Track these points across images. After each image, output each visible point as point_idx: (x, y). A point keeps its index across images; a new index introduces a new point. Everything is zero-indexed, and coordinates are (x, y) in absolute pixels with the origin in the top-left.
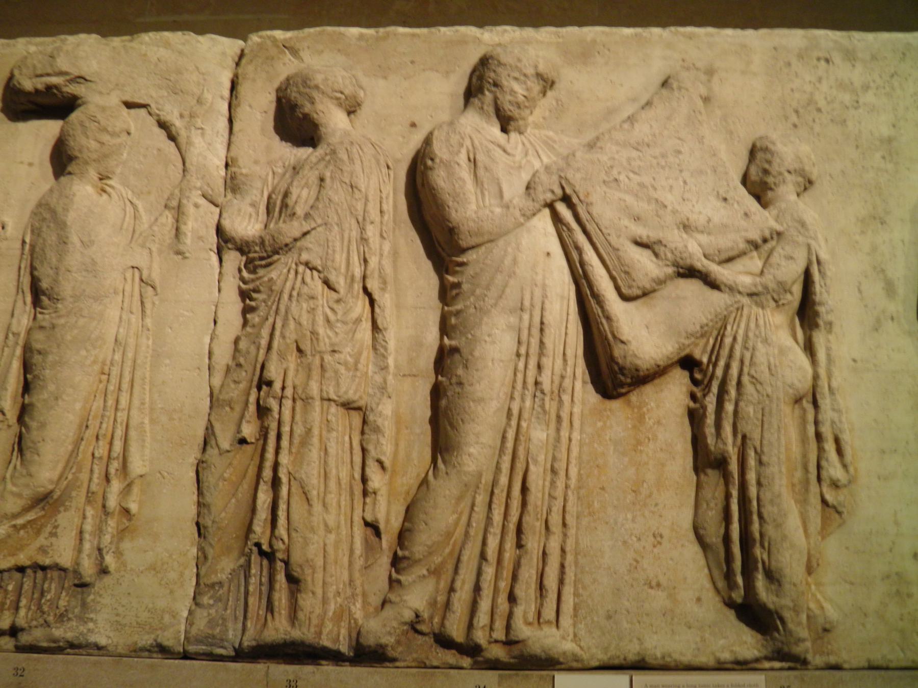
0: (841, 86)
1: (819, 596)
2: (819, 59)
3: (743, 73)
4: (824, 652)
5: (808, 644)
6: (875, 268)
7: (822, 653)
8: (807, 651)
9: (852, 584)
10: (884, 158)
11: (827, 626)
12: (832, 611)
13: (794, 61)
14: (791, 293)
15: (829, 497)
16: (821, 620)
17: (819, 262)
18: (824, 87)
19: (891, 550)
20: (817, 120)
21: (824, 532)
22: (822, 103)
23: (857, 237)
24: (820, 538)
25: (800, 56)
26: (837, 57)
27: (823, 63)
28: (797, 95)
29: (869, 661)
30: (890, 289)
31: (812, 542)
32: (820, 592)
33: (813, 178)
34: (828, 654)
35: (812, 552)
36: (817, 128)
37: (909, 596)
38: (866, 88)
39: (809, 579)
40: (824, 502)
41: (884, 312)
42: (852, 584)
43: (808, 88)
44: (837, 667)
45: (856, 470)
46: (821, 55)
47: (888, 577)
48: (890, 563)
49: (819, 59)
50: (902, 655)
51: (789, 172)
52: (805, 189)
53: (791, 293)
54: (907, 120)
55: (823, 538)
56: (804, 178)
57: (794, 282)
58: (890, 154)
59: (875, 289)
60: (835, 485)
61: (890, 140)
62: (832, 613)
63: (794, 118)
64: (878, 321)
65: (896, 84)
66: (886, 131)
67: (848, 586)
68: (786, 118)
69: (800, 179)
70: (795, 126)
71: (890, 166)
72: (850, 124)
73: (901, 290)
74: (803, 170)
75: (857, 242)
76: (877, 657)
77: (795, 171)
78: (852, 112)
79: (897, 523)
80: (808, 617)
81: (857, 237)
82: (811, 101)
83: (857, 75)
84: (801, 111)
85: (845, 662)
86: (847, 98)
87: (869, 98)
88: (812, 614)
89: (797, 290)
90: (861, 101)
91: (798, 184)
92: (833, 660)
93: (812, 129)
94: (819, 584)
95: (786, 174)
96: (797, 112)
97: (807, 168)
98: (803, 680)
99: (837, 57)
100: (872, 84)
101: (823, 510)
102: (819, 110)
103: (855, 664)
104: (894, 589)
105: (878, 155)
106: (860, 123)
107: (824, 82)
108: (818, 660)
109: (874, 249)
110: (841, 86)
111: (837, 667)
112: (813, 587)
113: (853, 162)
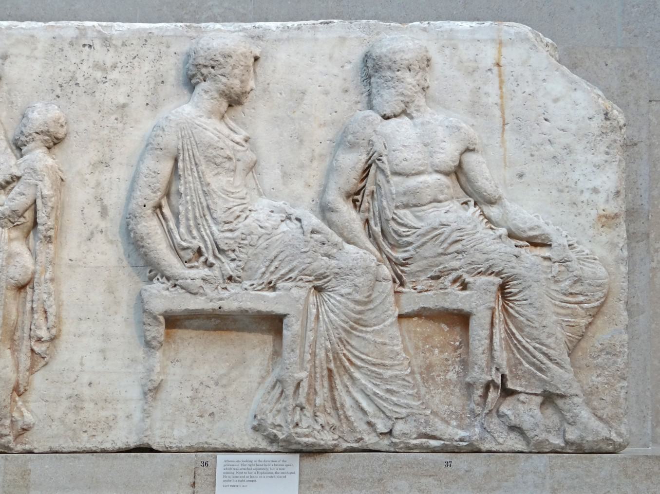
0: (97, 66)
1: (23, 409)
2: (84, 45)
3: (28, 57)
4: (22, 443)
5: (11, 438)
6: (96, 198)
7: (22, 443)
8: (9, 442)
9: (47, 401)
10: (116, 119)
11: (25, 427)
12: (31, 418)
13: (66, 47)
14: (24, 217)
15: (36, 349)
16: (20, 424)
17: (42, 197)
18: (84, 67)
19: (75, 381)
20: (74, 92)
21: (32, 370)
22: (80, 80)
23: (88, 176)
24: (28, 373)
25: (71, 44)
26: (97, 44)
27: (87, 47)
28: (63, 74)
29: (51, 448)
30: (104, 212)
31: (21, 375)
32: (26, 406)
33: (60, 136)
34: (26, 444)
35: (20, 382)
36: (73, 100)
37: (82, 409)
38: (114, 67)
39: (17, 398)
40: (32, 351)
41: (97, 227)
42: (47, 401)
43: (73, 68)
44: (31, 452)
45: (60, 330)
46: (86, 42)
47: (70, 397)
48: (73, 389)
49: (84, 45)
50: (72, 444)
51: (37, 133)
52: (55, 144)
53: (24, 217)
54: (138, 91)
55: (32, 374)
56: (50, 136)
57: (26, 210)
58: (122, 117)
59: (93, 212)
60: (39, 340)
61: (124, 106)
62: (29, 418)
63: (58, 91)
64: (92, 233)
65: (136, 64)
66: (122, 100)
67: (44, 403)
68: (53, 91)
69: (47, 138)
70: (59, 97)
71: (120, 125)
72: (96, 94)
73: (112, 213)
74: (48, 131)
75: (87, 180)
76: (56, 446)
77: (42, 132)
78: (101, 85)
79: (82, 364)
80: (12, 421)
81: (88, 176)
82: (72, 78)
83: (109, 58)
84: (64, 85)
85: (35, 448)
86: (99, 75)
87: (114, 75)
88: (14, 420)
89: (29, 215)
90: (108, 78)
91: (46, 141)
92: (27, 447)
93: (69, 99)
94: (25, 402)
95: (35, 135)
96: (61, 86)
97: (51, 130)
98: (7, 459)
99: (97, 44)
100: (119, 65)
101: (32, 355)
102: (77, 84)
103: (41, 450)
104: (73, 404)
105: (113, 117)
106: (105, 94)
107: (85, 63)
108: (19, 448)
109: (98, 184)
110: (97, 66)
111: (31, 452)
112: (20, 403)
113: (94, 123)
